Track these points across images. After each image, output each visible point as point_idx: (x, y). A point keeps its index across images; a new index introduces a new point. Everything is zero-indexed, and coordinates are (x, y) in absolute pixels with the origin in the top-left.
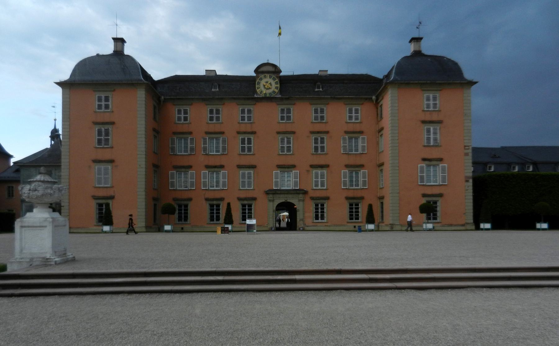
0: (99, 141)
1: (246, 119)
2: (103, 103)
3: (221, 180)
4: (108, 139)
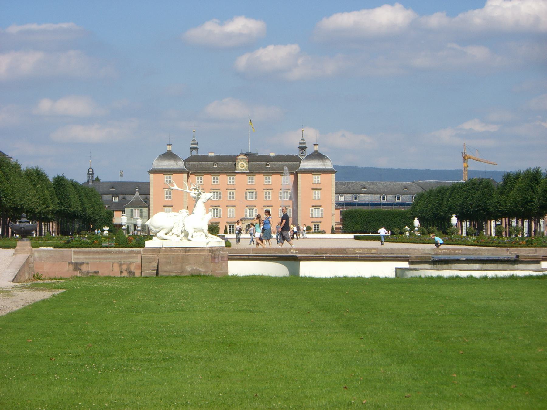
0: (167, 197)
1: (231, 182)
2: (168, 180)
3: (219, 213)
4: (170, 197)
